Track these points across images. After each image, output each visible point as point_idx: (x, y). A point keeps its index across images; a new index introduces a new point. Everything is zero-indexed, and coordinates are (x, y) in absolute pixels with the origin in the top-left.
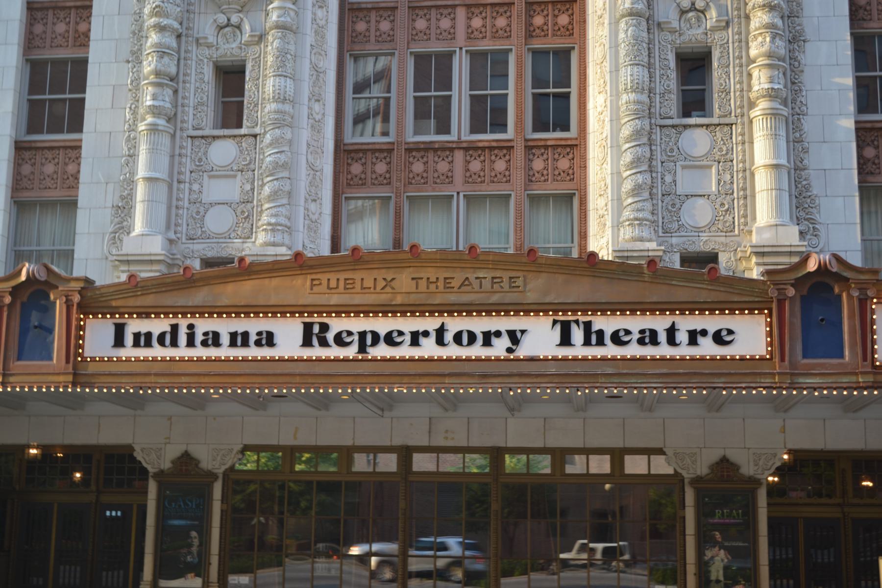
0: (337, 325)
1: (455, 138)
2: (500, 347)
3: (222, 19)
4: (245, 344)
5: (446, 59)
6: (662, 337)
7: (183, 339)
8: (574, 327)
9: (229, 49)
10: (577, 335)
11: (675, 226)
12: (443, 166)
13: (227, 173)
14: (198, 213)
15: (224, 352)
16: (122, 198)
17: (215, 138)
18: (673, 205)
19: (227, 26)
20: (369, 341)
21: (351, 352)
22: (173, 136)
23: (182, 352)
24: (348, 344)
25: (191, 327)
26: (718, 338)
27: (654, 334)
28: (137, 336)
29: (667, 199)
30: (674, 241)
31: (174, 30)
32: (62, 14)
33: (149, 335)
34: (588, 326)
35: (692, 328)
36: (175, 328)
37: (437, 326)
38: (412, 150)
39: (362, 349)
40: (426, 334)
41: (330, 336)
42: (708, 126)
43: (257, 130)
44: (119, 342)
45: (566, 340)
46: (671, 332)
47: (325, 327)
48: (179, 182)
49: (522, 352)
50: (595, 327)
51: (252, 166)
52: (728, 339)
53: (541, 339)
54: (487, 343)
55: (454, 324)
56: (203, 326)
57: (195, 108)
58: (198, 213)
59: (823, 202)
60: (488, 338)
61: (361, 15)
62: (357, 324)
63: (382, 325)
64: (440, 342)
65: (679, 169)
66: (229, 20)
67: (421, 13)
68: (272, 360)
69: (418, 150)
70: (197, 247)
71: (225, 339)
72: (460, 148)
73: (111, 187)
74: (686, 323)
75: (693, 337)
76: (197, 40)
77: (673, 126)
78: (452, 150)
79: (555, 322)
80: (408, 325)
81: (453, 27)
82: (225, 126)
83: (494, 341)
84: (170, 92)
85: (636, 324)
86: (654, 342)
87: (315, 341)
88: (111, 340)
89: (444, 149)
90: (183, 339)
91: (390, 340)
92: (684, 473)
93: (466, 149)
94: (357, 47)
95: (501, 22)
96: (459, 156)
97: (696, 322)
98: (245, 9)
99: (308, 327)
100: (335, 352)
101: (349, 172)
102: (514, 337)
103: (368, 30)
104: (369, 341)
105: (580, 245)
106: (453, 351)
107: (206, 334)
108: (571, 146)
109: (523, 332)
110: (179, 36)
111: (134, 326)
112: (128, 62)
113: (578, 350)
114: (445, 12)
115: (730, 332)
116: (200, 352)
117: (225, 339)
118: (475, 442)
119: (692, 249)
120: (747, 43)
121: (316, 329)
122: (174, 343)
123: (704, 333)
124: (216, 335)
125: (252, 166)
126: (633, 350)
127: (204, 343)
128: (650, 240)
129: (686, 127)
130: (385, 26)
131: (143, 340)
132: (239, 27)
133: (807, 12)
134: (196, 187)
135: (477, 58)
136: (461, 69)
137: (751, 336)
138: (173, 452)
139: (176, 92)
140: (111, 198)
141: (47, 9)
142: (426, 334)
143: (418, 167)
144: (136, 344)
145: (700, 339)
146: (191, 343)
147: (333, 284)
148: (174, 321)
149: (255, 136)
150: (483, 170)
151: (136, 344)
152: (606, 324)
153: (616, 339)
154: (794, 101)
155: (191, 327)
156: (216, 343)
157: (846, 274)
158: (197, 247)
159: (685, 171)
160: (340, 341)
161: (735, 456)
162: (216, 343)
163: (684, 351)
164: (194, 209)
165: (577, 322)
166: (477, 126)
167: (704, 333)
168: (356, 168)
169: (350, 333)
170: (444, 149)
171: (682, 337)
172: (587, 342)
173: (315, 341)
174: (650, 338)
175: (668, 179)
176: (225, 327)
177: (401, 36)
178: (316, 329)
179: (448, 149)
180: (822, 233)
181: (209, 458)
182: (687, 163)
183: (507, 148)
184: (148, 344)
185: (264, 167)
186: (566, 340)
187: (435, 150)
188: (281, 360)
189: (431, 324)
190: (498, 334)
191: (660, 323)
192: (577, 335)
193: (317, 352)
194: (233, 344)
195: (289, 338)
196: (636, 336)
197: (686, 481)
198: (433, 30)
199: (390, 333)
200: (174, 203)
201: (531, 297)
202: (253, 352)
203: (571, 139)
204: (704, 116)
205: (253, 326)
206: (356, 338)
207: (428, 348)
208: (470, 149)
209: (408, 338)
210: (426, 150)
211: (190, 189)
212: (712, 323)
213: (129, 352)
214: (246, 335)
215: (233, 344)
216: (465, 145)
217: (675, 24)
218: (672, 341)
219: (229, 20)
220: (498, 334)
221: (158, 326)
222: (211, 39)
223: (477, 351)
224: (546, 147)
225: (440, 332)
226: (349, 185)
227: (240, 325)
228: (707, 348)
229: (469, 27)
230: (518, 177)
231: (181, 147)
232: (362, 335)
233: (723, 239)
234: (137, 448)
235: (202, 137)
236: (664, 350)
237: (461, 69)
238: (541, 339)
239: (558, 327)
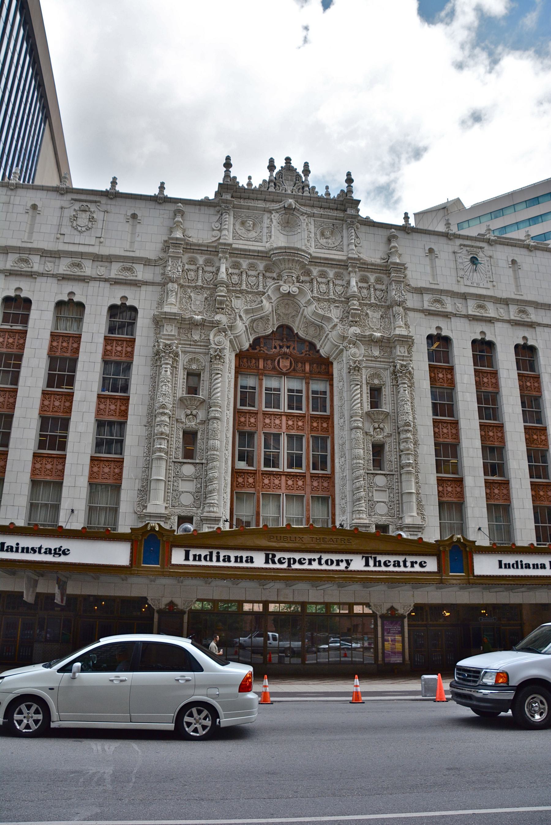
0: (279, 555)
1: (282, 470)
2: (343, 566)
3: (189, 412)
4: (241, 561)
5: (277, 437)
6: (402, 564)
7: (214, 558)
8: (370, 559)
9: (192, 424)
10: (371, 562)
11: (373, 514)
12: (277, 482)
13: (186, 479)
14: (177, 495)
15: (232, 564)
16: (143, 487)
17: (184, 463)
18: (372, 505)
19: (190, 415)
20: (292, 562)
21: (285, 566)
22: (167, 461)
23: (214, 563)
24: (284, 563)
25: (218, 553)
26: (421, 565)
27: (399, 562)
28: (195, 556)
29: (370, 502)
30: (373, 519)
31: (169, 415)
32: (113, 401)
33: (200, 556)
34: (375, 558)
35: (412, 560)
36: (211, 554)
37: (319, 557)
38: (264, 473)
39: (289, 565)
40: (314, 560)
41: (276, 559)
42: (384, 475)
43: (204, 461)
44: (187, 558)
45: (367, 564)
46: (405, 562)
47: (274, 556)
48: (169, 481)
49: (351, 568)
50: (378, 560)
51: (201, 477)
52: (424, 565)
53: (358, 564)
54: (338, 564)
55: (325, 557)
56: (223, 553)
57: (176, 449)
58: (177, 495)
59: (425, 507)
60: (338, 563)
61: (242, 414)
62: (287, 555)
63: (297, 556)
64: (320, 563)
65: (374, 491)
66: (191, 412)
67: (267, 416)
68: (251, 568)
69: (266, 474)
70: (176, 511)
71: (233, 559)
72: (283, 475)
73: (137, 481)
74: (410, 559)
75: (413, 564)
76: (177, 419)
77: (372, 474)
78: (280, 475)
79: (363, 557)
80: (308, 556)
81: (281, 423)
82: (185, 457)
83: (340, 564)
84: (166, 441)
85: (392, 559)
86: (399, 566)
87: (270, 561)
88: (183, 557)
89: (277, 475)
90: (214, 558)
91: (300, 562)
92: (377, 613)
93: (286, 475)
94: (241, 427)
95: (300, 423)
96: (283, 478)
97: (414, 559)
98: (198, 408)
99: (267, 556)
100: (278, 566)
101: (237, 481)
102: (348, 562)
103: (245, 421)
104: (292, 562)
105: (332, 518)
106: (324, 567)
107: (224, 556)
108: (328, 477)
109: (351, 560)
110: (169, 418)
111: (192, 552)
112: (146, 426)
113: (372, 568)
114: (278, 417)
115: (425, 562)
116: (221, 564)
117: (233, 559)
118: (296, 599)
119: (379, 523)
120: (399, 443)
121: (270, 556)
122: (211, 560)
123: (416, 562)
124: (229, 557)
125: (201, 477)
126: (391, 568)
127: (224, 561)
128: (366, 519)
129: (377, 474)
130: (252, 420)
131: (197, 558)
132: (195, 416)
133: (419, 433)
134: (175, 484)
135: (290, 437)
136: (284, 440)
137: (432, 565)
138: (165, 601)
139: (168, 441)
140: (138, 485)
141: (107, 398)
142: (314, 560)
143: (266, 481)
144: (194, 559)
145: (415, 565)
146: (218, 560)
147: (279, 539)
148: (211, 550)
149: (202, 464)
150: (293, 484)
151: (194, 559)
152: (382, 559)
153: (386, 565)
154: (416, 467)
155: (218, 553)
156: (229, 561)
157: (466, 543)
158: (176, 511)
159: (377, 492)
160: (280, 562)
161: (396, 606)
162: (229, 561)
163: (409, 569)
164: (174, 492)
165: (371, 557)
166: (290, 466)
167: (416, 562)
168: (240, 480)
169: (284, 559)
170: (277, 475)
171: (408, 564)
172: (375, 565)
173: (270, 561)
174: (397, 564)
175: (370, 495)
176: (233, 554)
177: (260, 425)
178: (270, 556)
179: (278, 475)
180: (427, 519)
181: (180, 604)
182: (377, 489)
183: (302, 476)
184: (200, 560)
185: (208, 478)
186: (367, 564)
187: (274, 475)
188: (255, 568)
189: (316, 556)
190: (342, 561)
191: (401, 559)
192: (371, 562)
193: (271, 566)
194: (236, 561)
195: (259, 560)
196: (392, 563)
197: (378, 616)
198: (273, 424)
199: (301, 559)
200: (167, 491)
201: (354, 547)
202: (244, 565)
203: (328, 474)
204: (380, 470)
205: (245, 554)
206: (287, 560)
207: (315, 566)
208: (289, 475)
209: (307, 561)
210: (270, 474)
211: (173, 485)
212: (419, 559)
213: (191, 562)
214: (241, 558)
215: (236, 561)
216: (286, 473)
217: (372, 433)
218: (405, 566)
219: (191, 412)
220: (342, 561)
221: (204, 552)
222: (184, 420)
223: (334, 567)
224: (319, 477)
225: (320, 559)
226: (237, 486)
227: (239, 554)
228: (417, 568)
229: (287, 424)
230: (308, 489)
231: (170, 466)
232: (289, 559)
233: (391, 520)
234: (149, 599)
235: (179, 462)
236: (402, 569)
237: (284, 440)
238: (358, 564)
239: (364, 559)
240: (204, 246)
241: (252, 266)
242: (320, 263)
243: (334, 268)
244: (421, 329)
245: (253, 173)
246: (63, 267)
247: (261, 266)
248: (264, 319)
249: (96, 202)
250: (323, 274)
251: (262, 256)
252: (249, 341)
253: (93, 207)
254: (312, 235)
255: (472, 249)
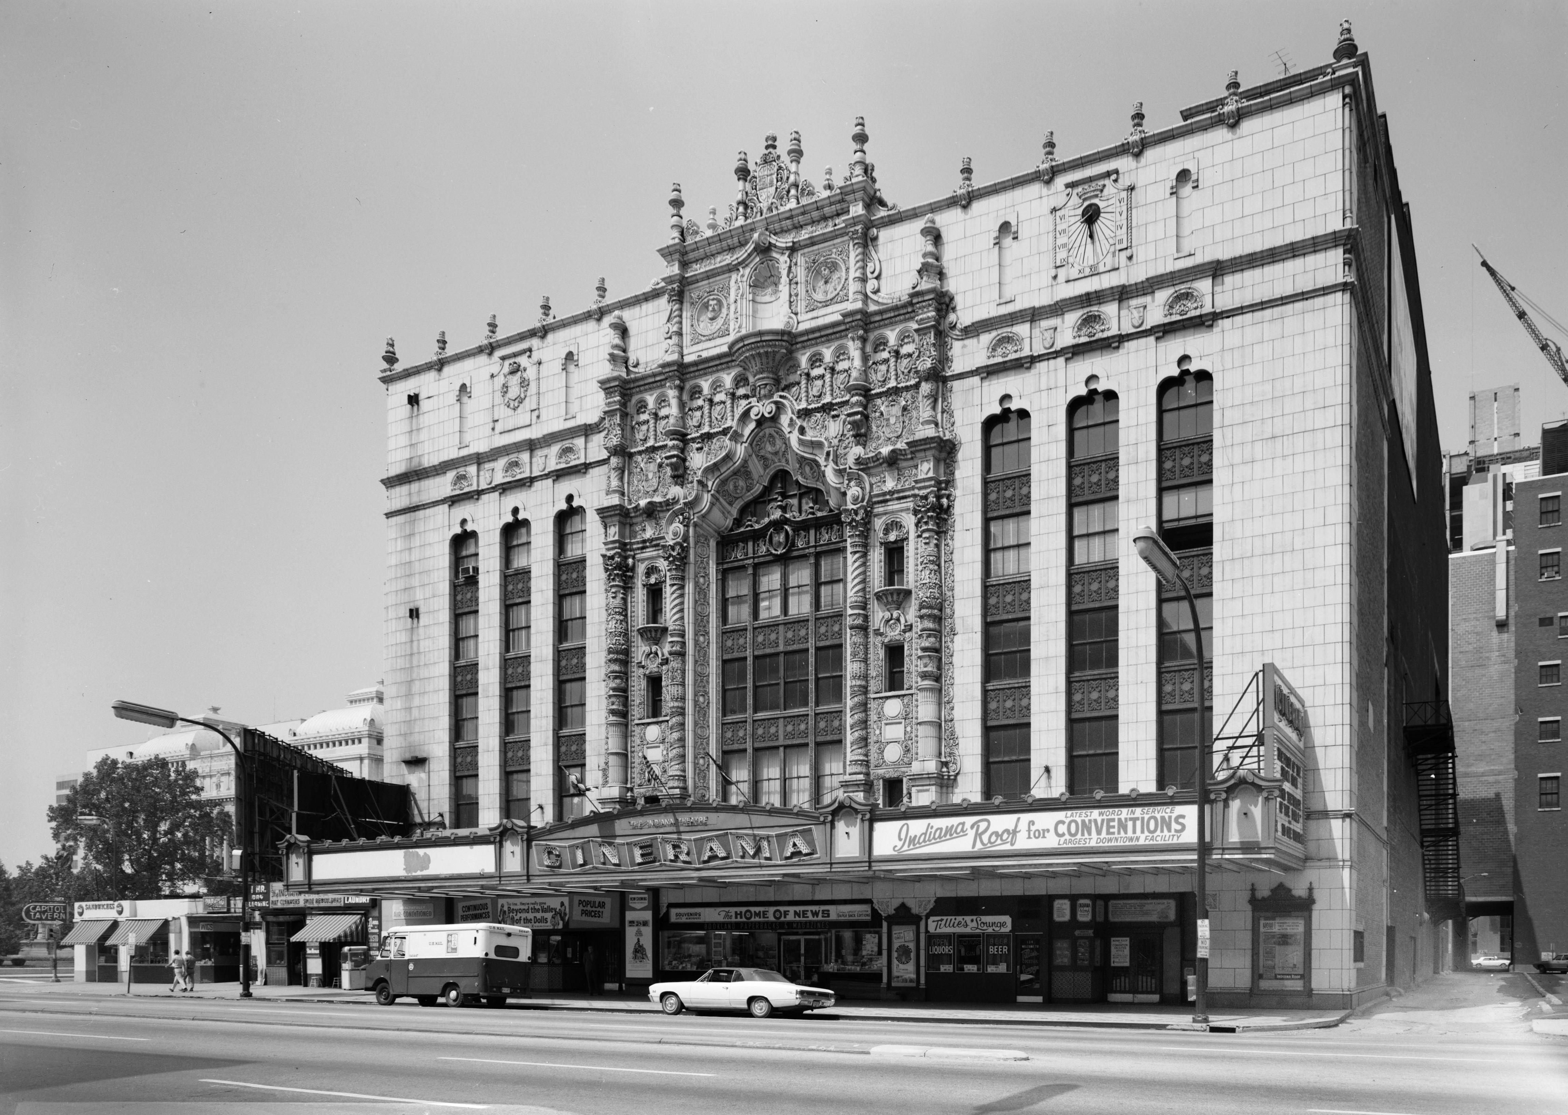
240: (649, 376)
241: (716, 386)
242: (809, 340)
243: (832, 340)
244: (970, 408)
245: (714, 205)
246: (497, 472)
247: (727, 379)
248: (743, 471)
249: (523, 352)
250: (816, 360)
251: (727, 363)
252: (732, 515)
253: (523, 360)
254: (801, 289)
255: (1086, 187)
